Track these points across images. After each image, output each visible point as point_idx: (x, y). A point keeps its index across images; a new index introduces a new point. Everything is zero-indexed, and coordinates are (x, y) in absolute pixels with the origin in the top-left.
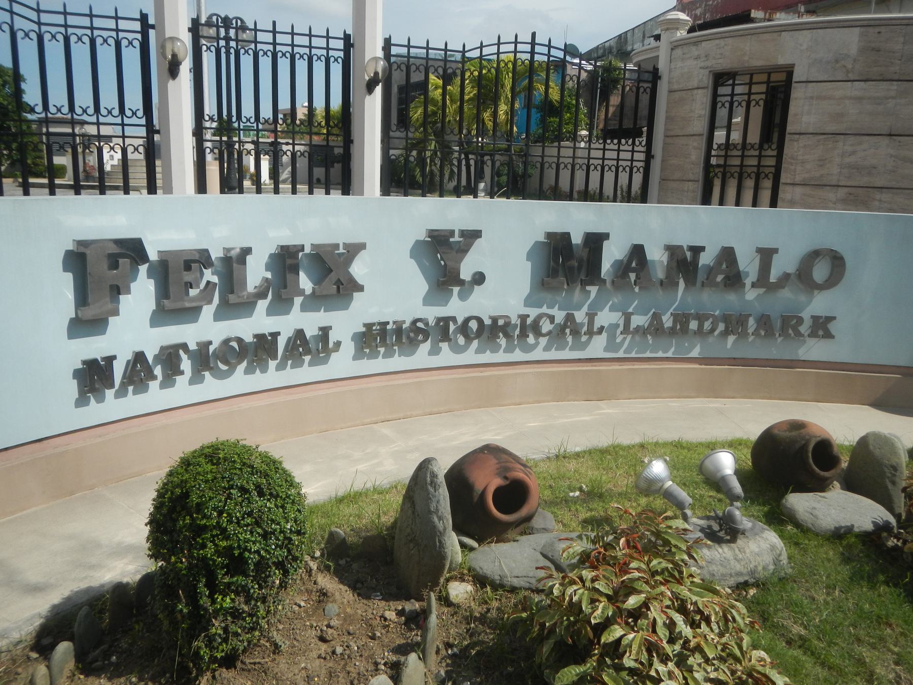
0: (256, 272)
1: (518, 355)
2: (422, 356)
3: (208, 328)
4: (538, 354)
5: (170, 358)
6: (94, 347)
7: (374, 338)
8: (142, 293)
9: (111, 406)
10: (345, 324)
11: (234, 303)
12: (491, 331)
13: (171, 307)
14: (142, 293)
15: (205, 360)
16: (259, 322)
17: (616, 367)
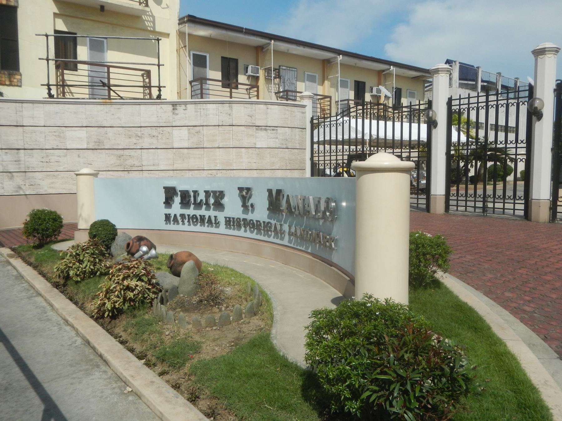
0: (202, 197)
1: (266, 238)
2: (242, 232)
3: (191, 211)
4: (271, 239)
5: (183, 216)
6: (168, 211)
7: (229, 222)
8: (177, 200)
9: (172, 226)
10: (221, 216)
11: (198, 205)
12: (254, 226)
13: (185, 203)
14: (177, 200)
15: (194, 219)
16: (203, 212)
17: (292, 251)
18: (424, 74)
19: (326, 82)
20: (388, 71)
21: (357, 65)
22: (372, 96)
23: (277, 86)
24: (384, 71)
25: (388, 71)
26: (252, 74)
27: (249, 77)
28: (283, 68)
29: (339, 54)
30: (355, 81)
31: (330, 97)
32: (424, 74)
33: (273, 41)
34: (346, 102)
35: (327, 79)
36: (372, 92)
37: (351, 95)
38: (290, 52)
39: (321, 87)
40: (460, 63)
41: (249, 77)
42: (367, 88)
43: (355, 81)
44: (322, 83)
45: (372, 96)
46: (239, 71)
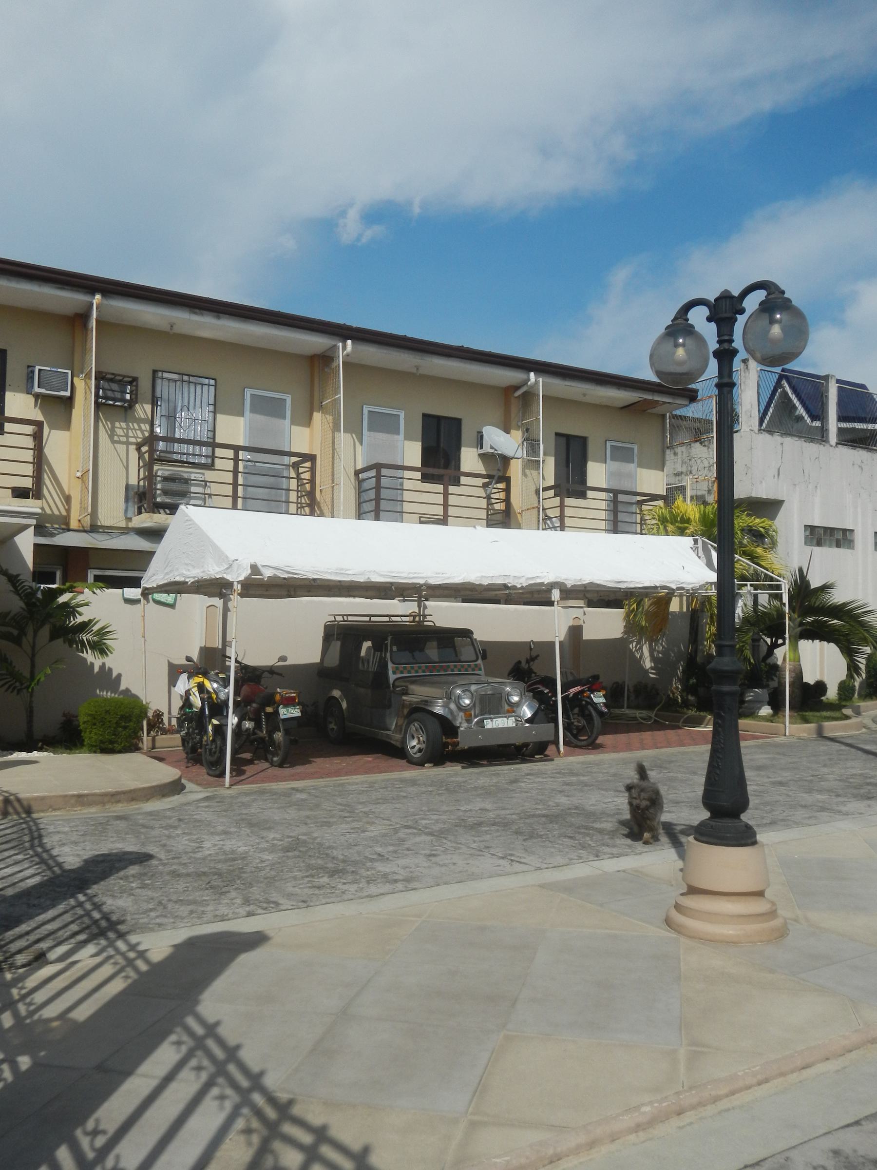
18: (649, 397)
19: (317, 416)
20: (524, 389)
21: (421, 371)
22: (481, 456)
23: (146, 427)
24: (517, 388)
25: (524, 389)
26: (43, 391)
27: (37, 396)
28: (165, 375)
29: (344, 338)
30: (425, 416)
31: (312, 458)
32: (649, 397)
33: (98, 297)
34: (373, 473)
35: (321, 408)
36: (482, 448)
37: (412, 453)
38: (177, 330)
39: (306, 431)
40: (838, 381)
41: (37, 396)
42: (467, 433)
43: (425, 416)
44: (307, 422)
45: (484, 457)
46: (8, 381)
